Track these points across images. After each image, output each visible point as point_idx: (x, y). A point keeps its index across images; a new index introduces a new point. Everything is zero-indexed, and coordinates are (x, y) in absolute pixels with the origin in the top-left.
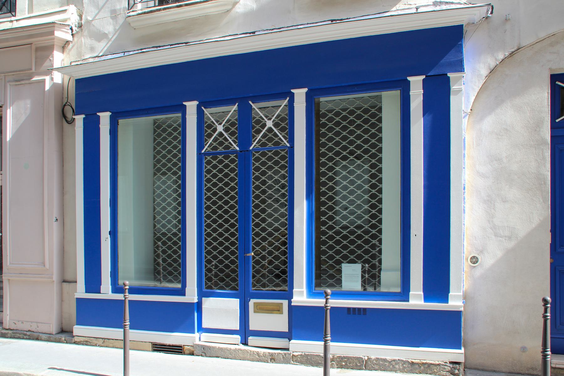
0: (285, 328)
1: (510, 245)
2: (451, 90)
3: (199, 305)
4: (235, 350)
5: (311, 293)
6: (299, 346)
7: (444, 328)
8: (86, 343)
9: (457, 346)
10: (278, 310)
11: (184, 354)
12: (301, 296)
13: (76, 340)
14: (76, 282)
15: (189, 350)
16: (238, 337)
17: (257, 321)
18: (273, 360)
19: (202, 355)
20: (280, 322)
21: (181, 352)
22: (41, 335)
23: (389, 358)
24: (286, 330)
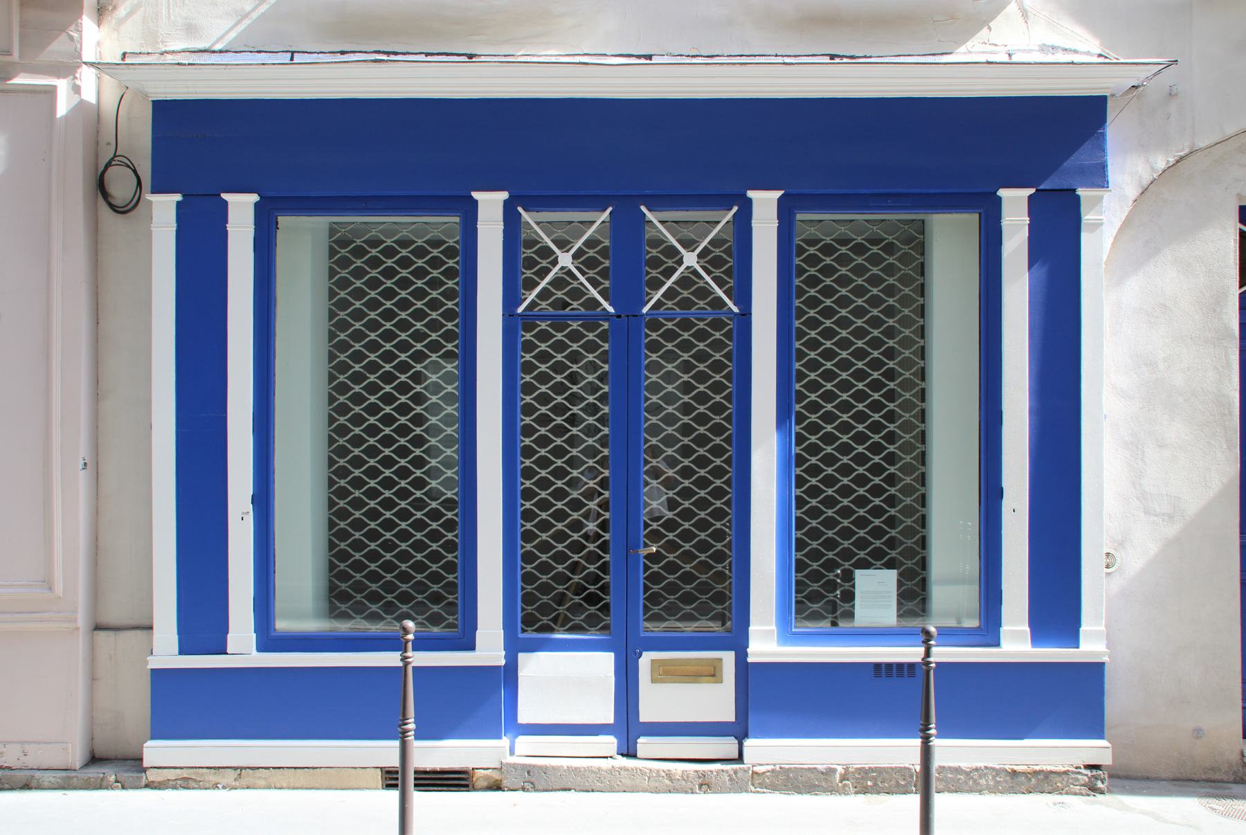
1: (1171, 530)
2: (1084, 222)
3: (509, 673)
4: (612, 771)
5: (787, 635)
6: (764, 751)
8: (185, 783)
10: (712, 673)
11: (474, 789)
12: (766, 642)
13: (151, 778)
14: (151, 628)
15: (487, 778)
19: (523, 789)
20: (717, 701)
22: (38, 774)
23: (965, 765)
24: (731, 717)
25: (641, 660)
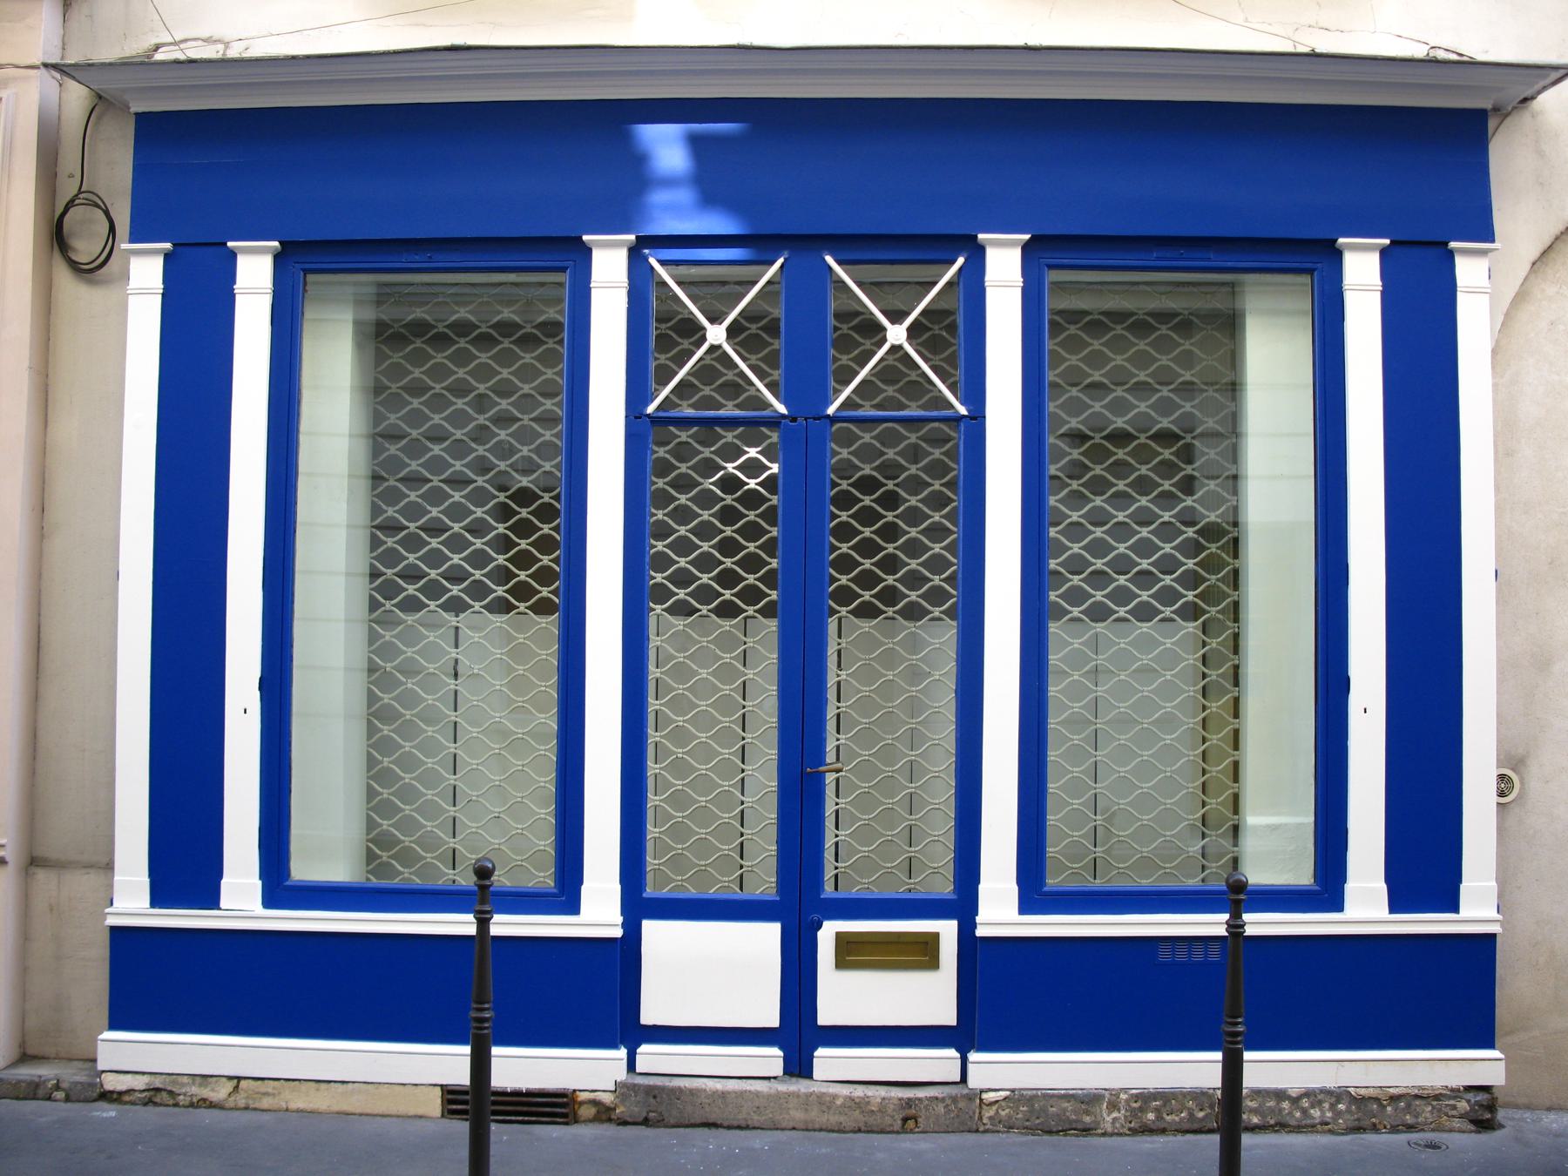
0: (945, 1013)
7: (1444, 990)
9: (1481, 1034)
10: (923, 953)
16: (776, 1051)
17: (843, 996)
18: (911, 1123)
20: (932, 996)
21: (565, 1115)
25: (819, 933)
